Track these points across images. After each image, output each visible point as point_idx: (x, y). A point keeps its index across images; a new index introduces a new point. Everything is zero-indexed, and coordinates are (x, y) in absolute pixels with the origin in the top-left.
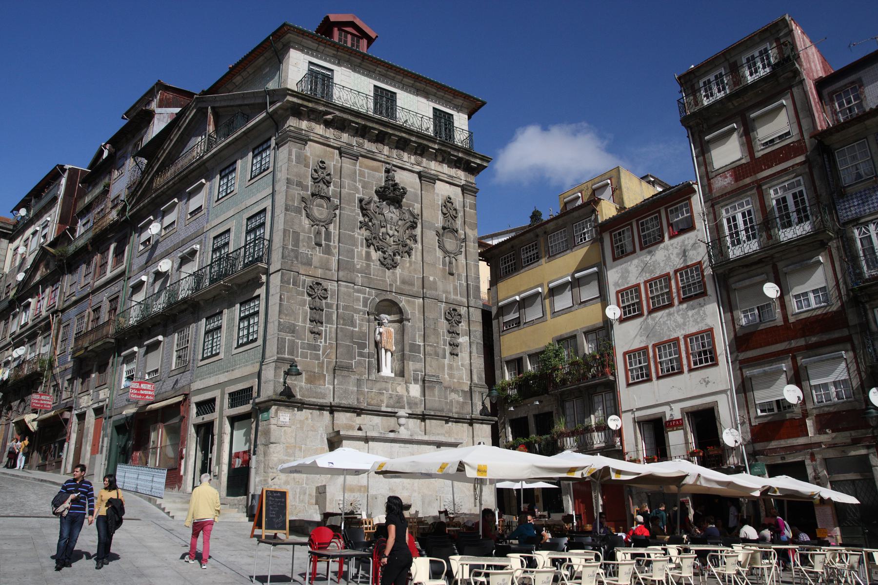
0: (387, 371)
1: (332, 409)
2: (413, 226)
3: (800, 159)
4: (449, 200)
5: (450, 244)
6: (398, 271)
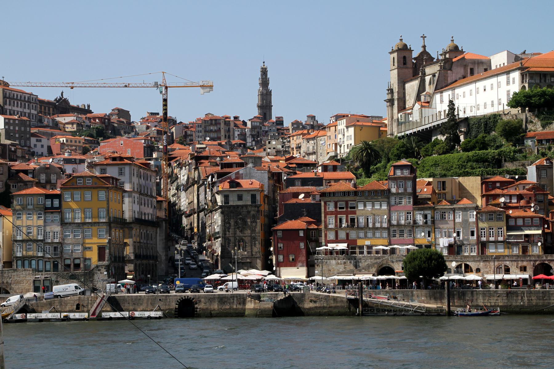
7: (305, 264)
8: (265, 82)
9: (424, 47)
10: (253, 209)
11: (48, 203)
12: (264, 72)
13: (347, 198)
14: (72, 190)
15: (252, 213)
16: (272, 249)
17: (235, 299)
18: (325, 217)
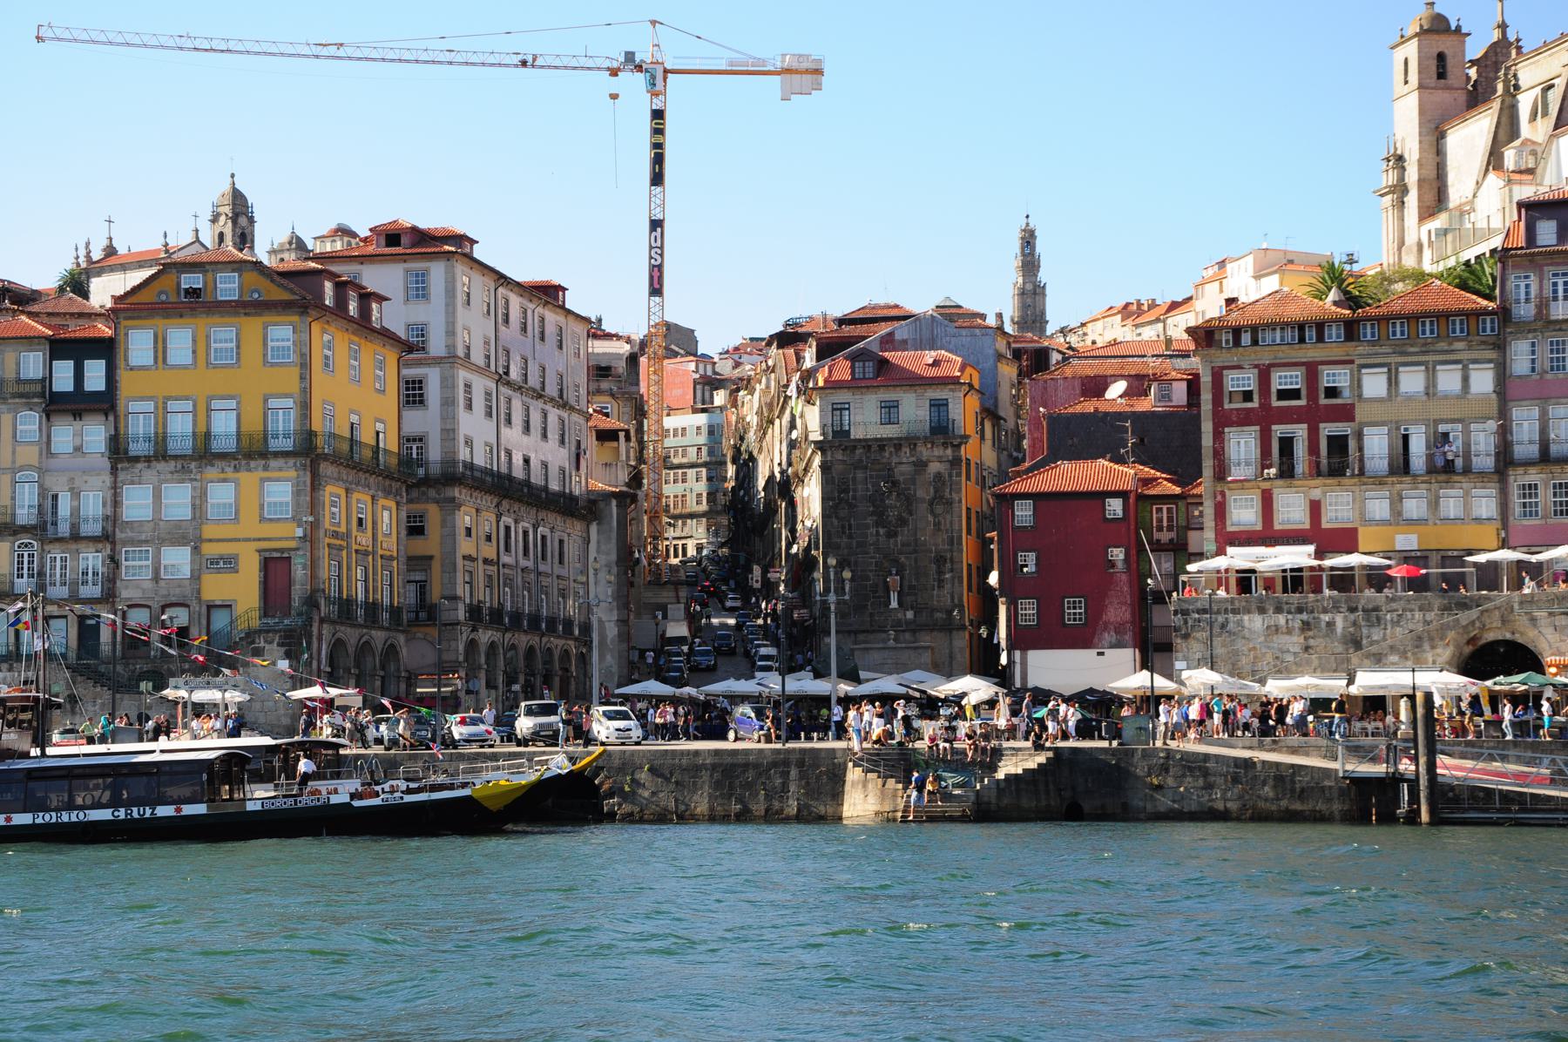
0: (894, 604)
1: (856, 633)
5: (939, 509)
7: (1128, 637)
8: (1030, 264)
9: (1503, 26)
10: (938, 452)
11: (63, 376)
12: (1029, 239)
13: (1311, 352)
14: (160, 322)
15: (934, 467)
16: (993, 579)
17: (794, 773)
18: (1218, 435)
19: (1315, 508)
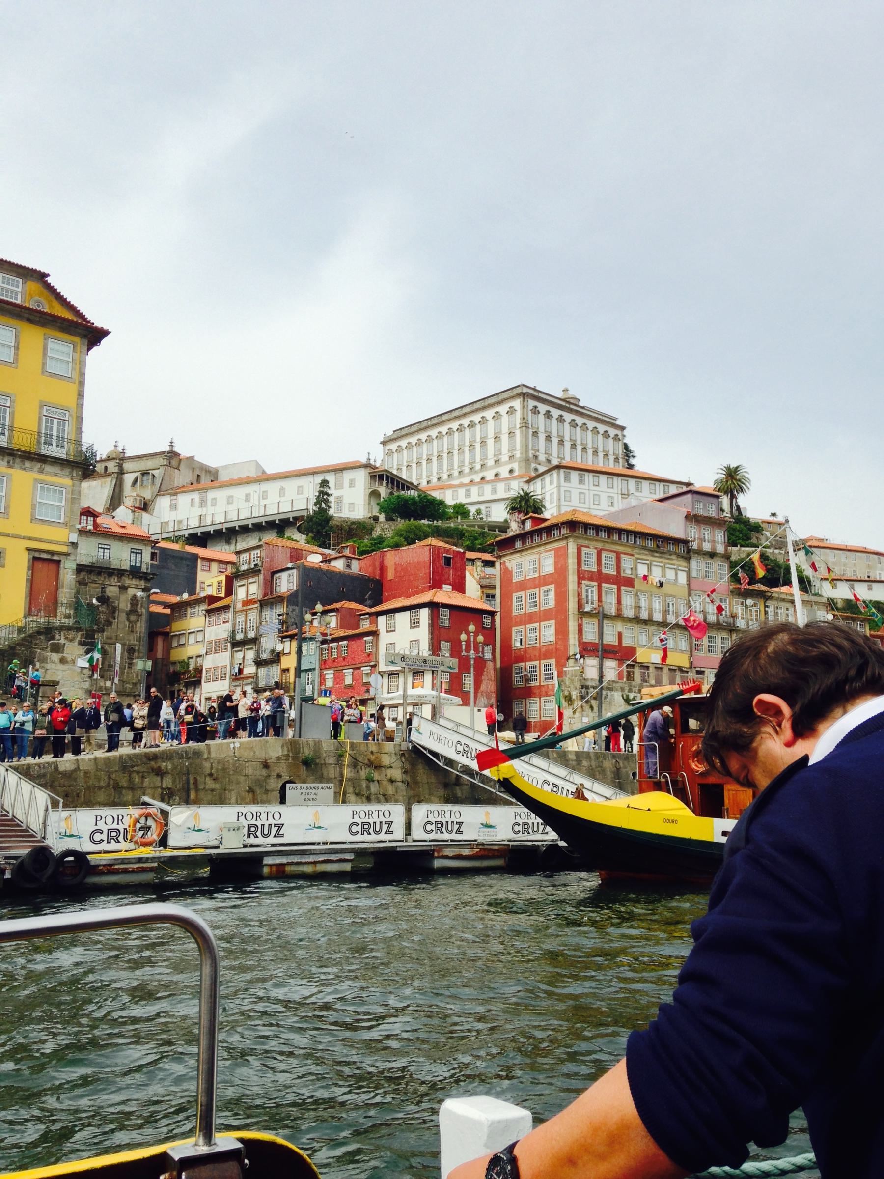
2: (114, 612)
3: (256, 606)
4: (135, 596)
5: (133, 618)
6: (105, 633)
10: (134, 582)
19: (620, 635)
